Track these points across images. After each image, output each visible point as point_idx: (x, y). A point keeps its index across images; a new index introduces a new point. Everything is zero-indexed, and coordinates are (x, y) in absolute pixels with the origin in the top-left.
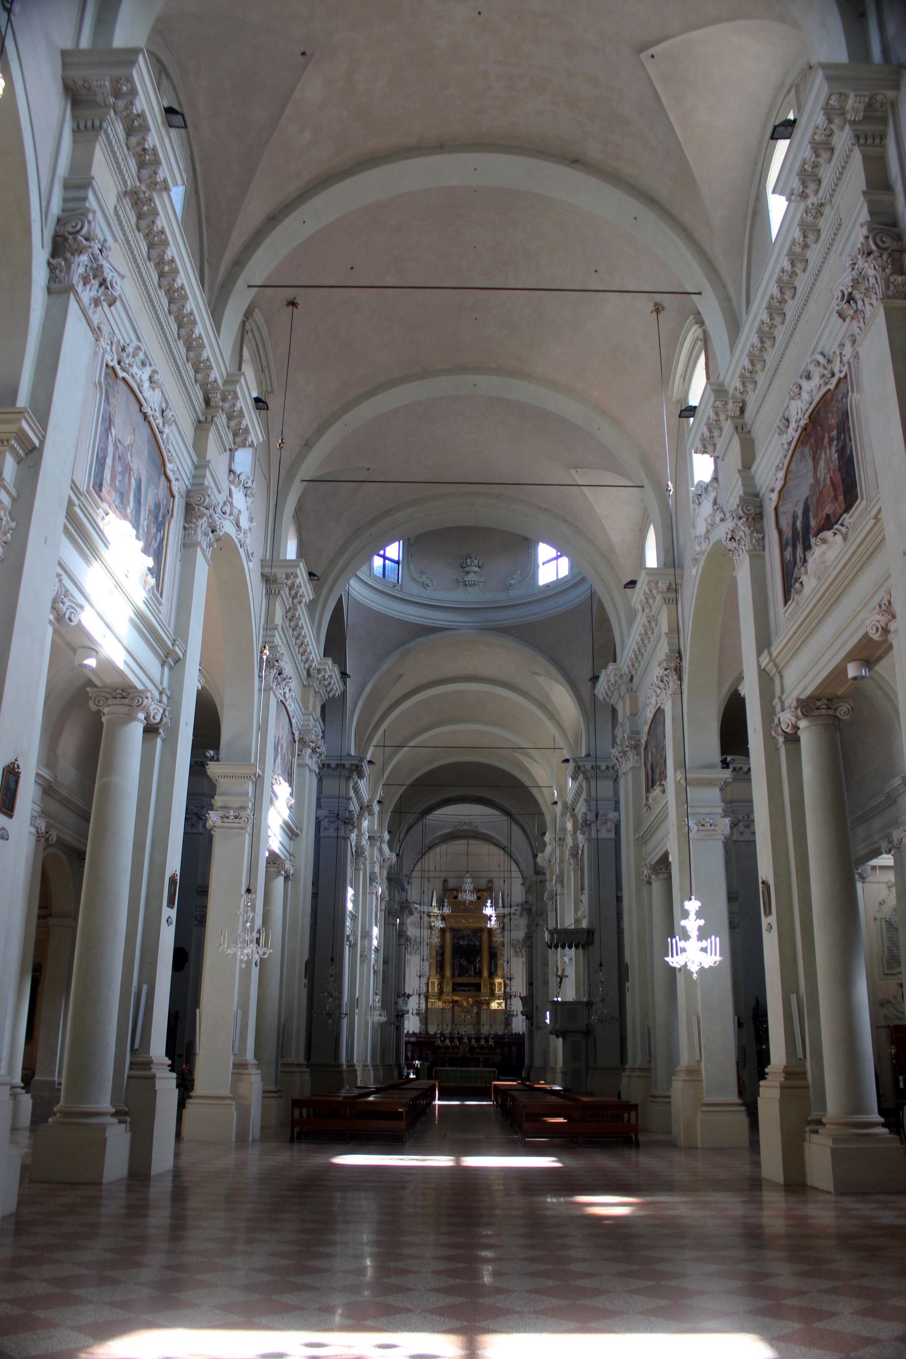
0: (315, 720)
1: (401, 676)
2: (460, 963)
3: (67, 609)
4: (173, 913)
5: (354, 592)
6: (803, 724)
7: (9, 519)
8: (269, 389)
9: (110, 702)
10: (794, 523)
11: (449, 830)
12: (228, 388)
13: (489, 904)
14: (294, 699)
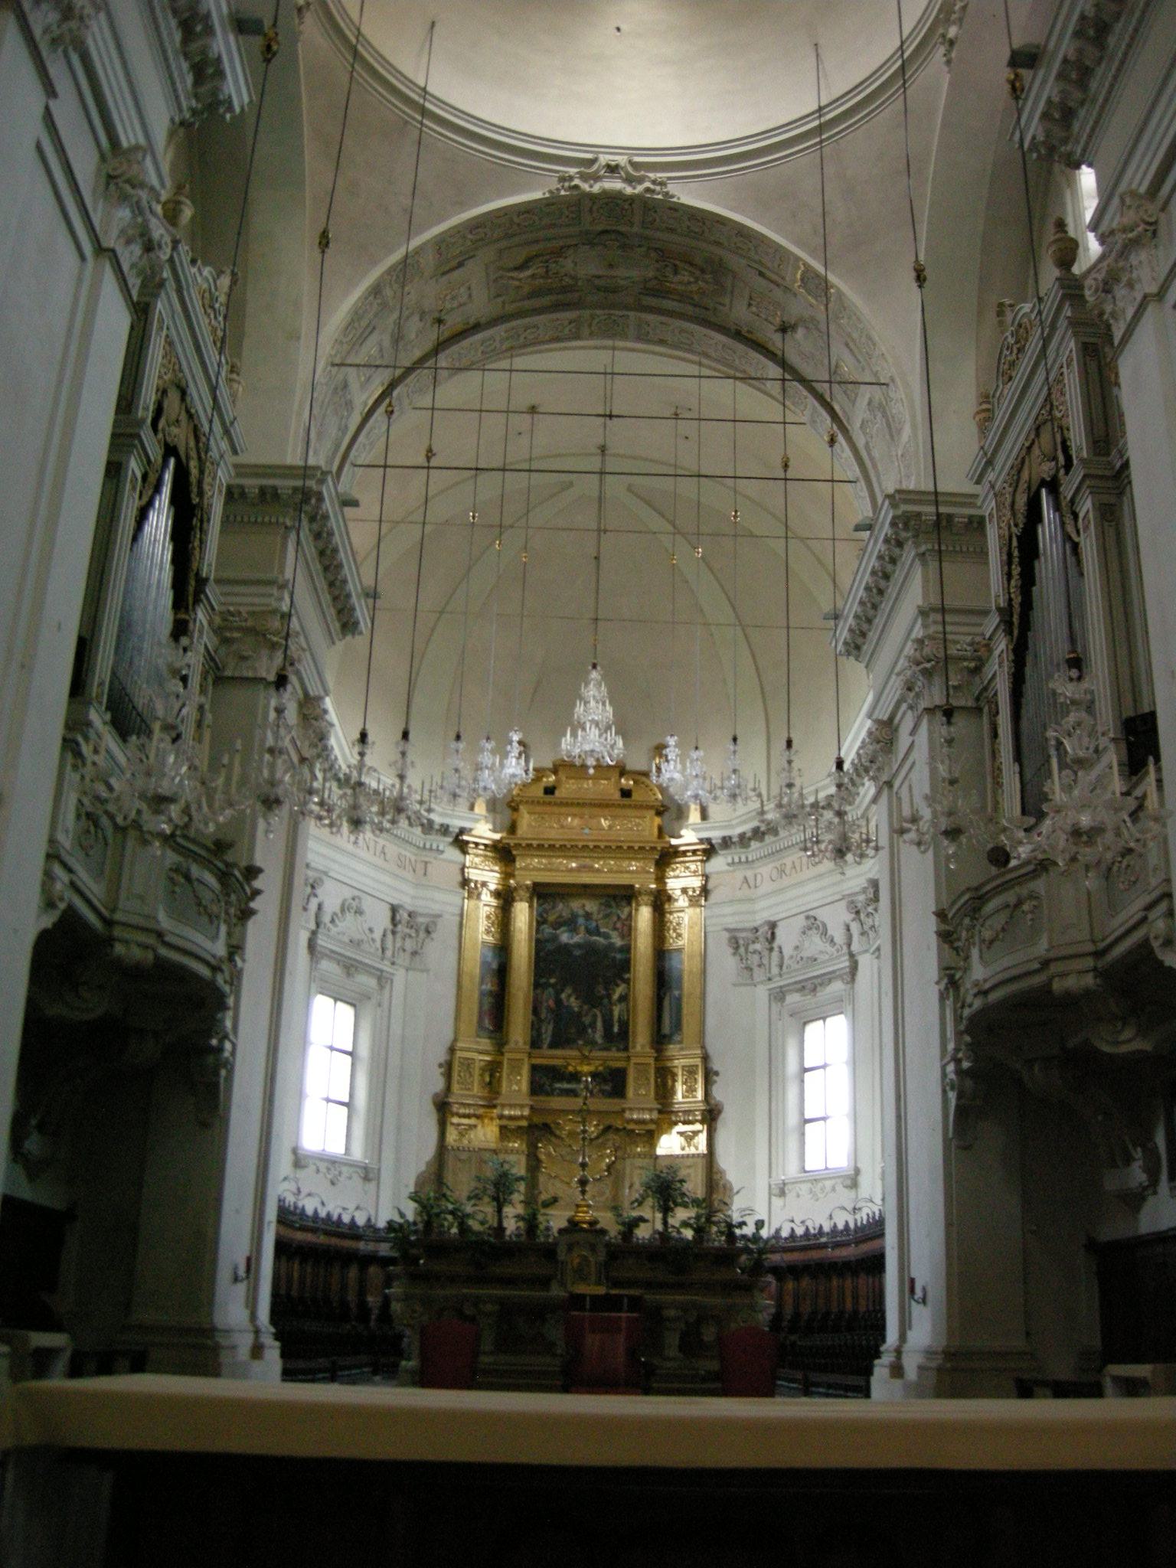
2: (558, 1002)
13: (672, 753)
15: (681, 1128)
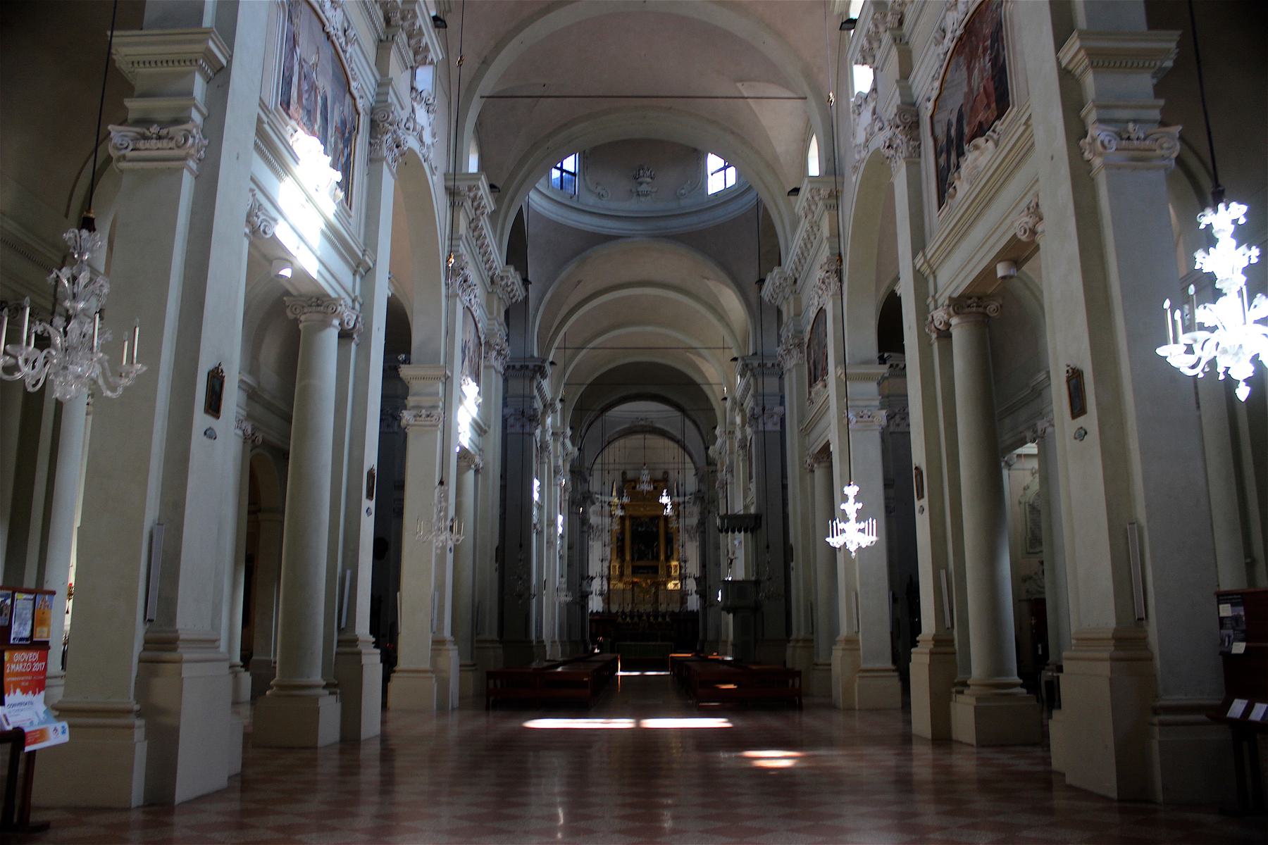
0: (500, 325)
1: (579, 282)
3: (261, 223)
4: (372, 504)
5: (533, 203)
6: (954, 321)
7: (201, 137)
8: (447, 8)
9: (306, 310)
10: (949, 130)
11: (627, 426)
12: (408, 7)
13: (664, 494)
14: (480, 305)
15: (673, 582)
